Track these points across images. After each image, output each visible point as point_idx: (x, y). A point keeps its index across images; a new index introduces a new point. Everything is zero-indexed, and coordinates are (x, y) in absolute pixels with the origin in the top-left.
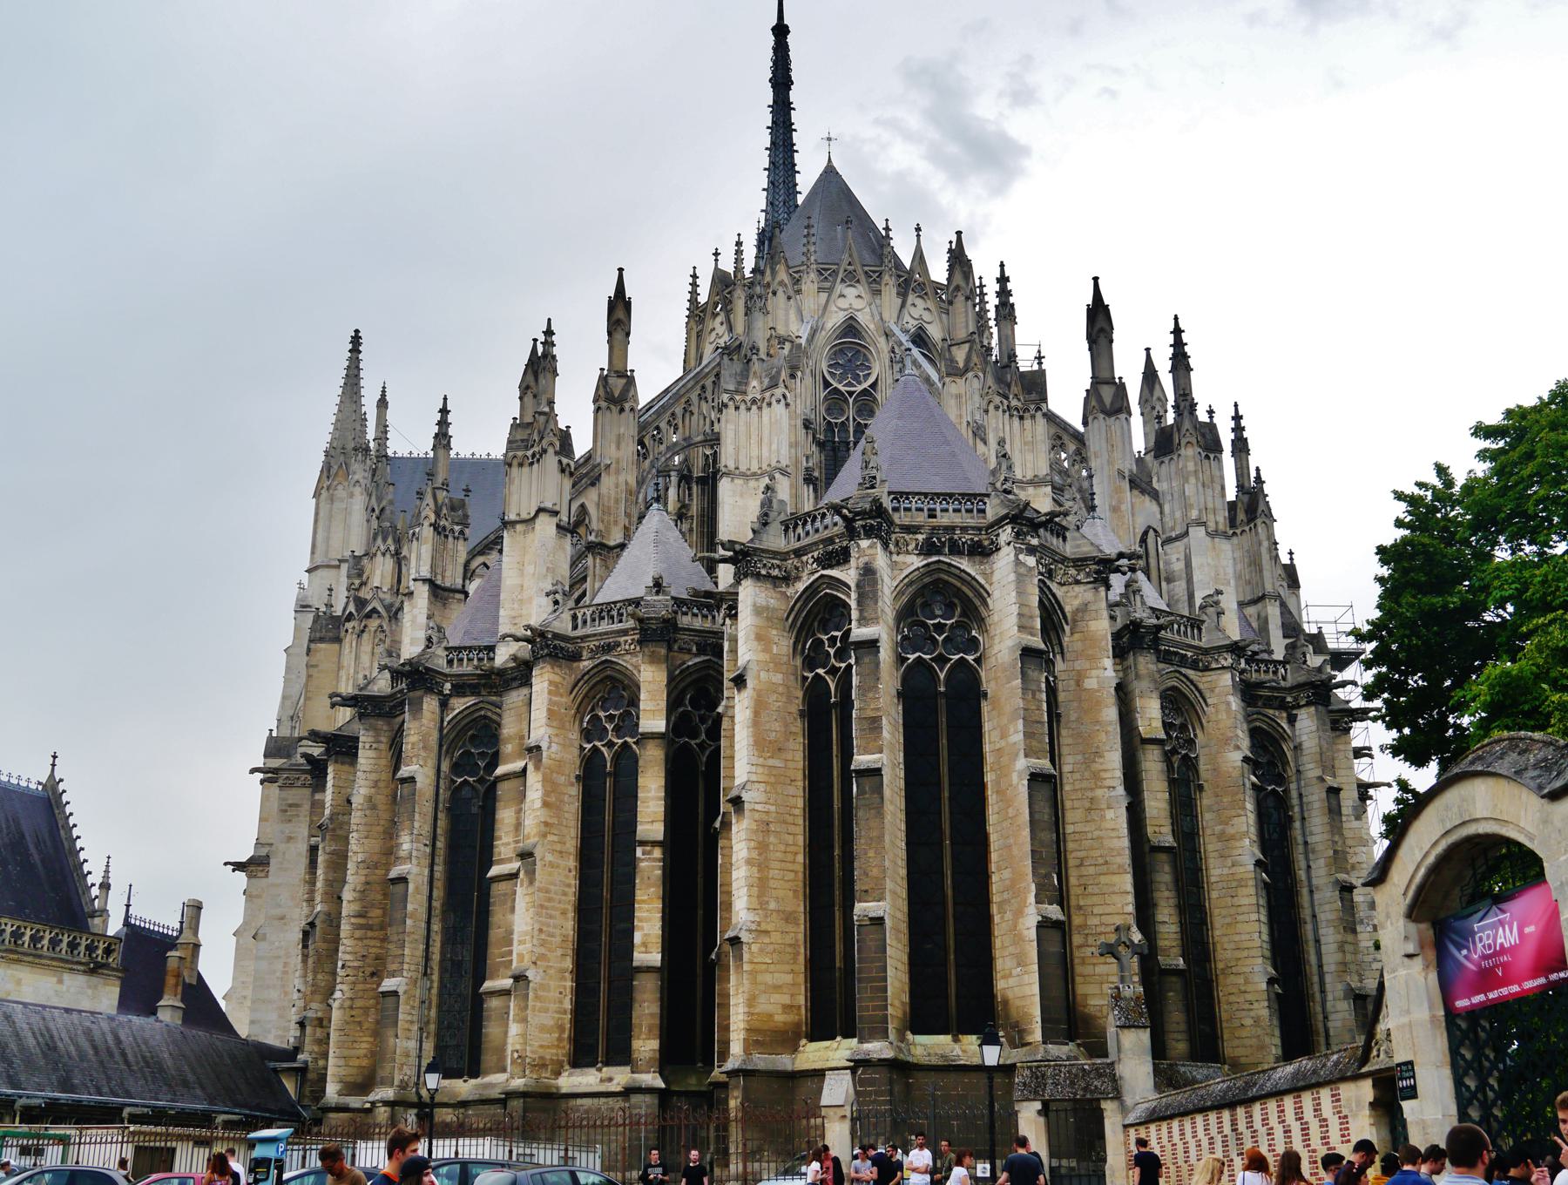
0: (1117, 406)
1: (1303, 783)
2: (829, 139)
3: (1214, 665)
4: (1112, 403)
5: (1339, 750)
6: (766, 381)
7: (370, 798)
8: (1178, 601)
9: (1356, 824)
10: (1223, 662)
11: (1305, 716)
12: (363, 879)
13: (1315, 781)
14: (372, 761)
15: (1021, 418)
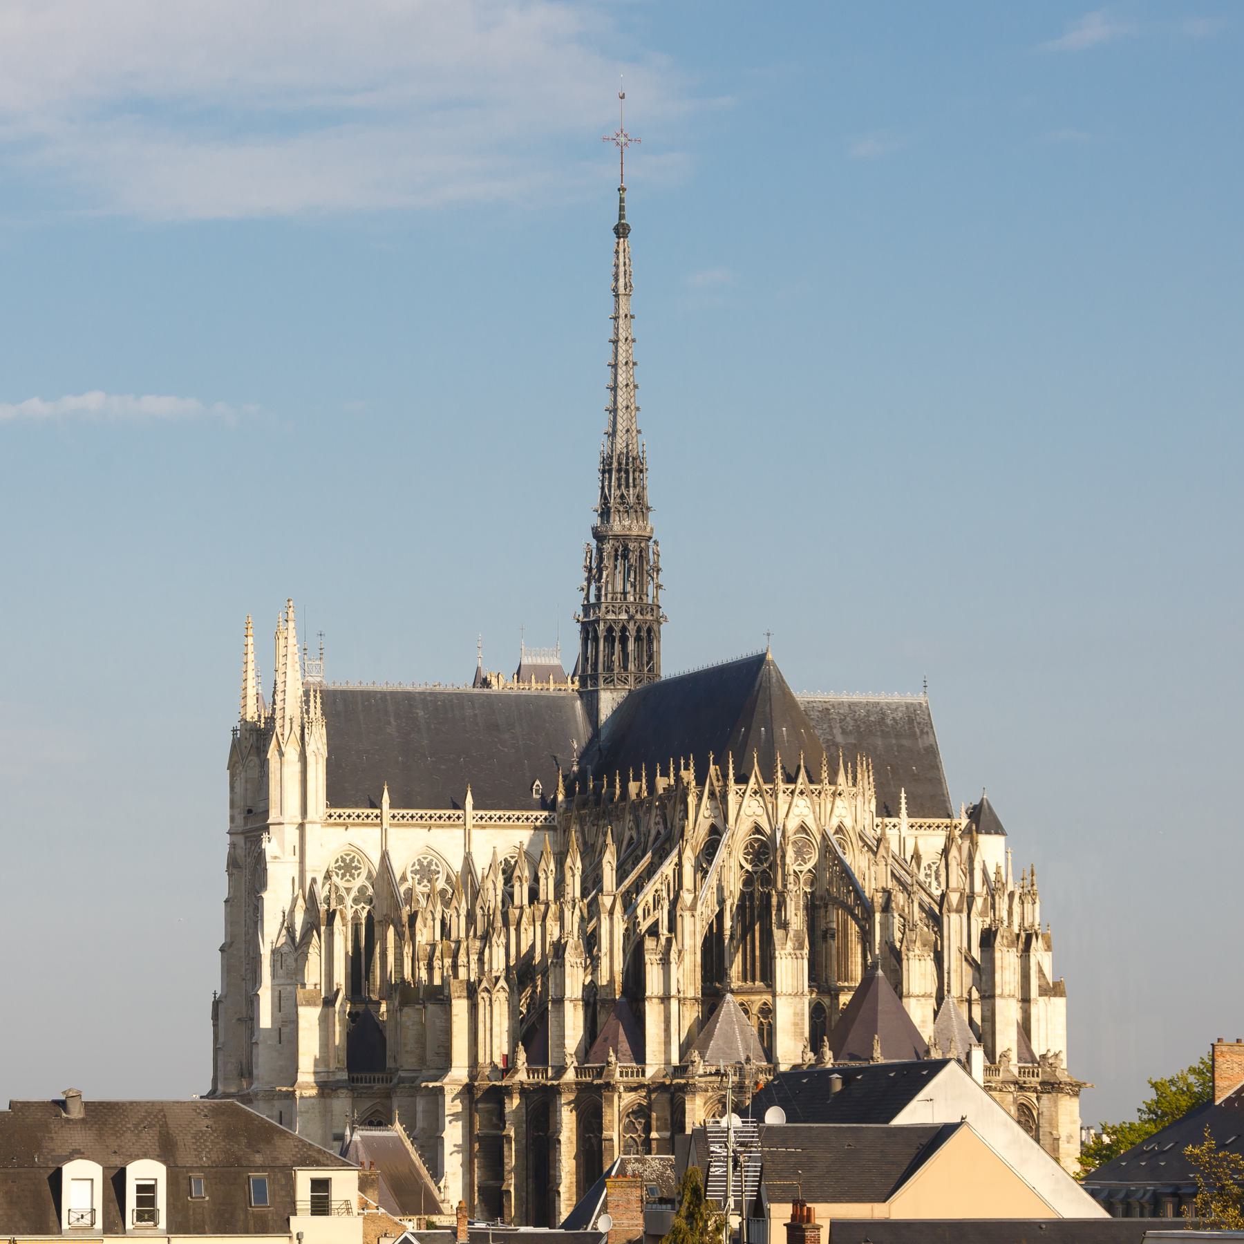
0: (959, 908)
1: (1041, 1133)
2: (768, 635)
3: (1004, 1090)
4: (957, 905)
5: (1062, 1104)
6: (797, 944)
7: (570, 1137)
8: (986, 1033)
9: (1067, 1145)
10: (1009, 1089)
11: (1046, 1098)
12: (569, 1180)
13: (1048, 1134)
14: (569, 1118)
15: (920, 960)
